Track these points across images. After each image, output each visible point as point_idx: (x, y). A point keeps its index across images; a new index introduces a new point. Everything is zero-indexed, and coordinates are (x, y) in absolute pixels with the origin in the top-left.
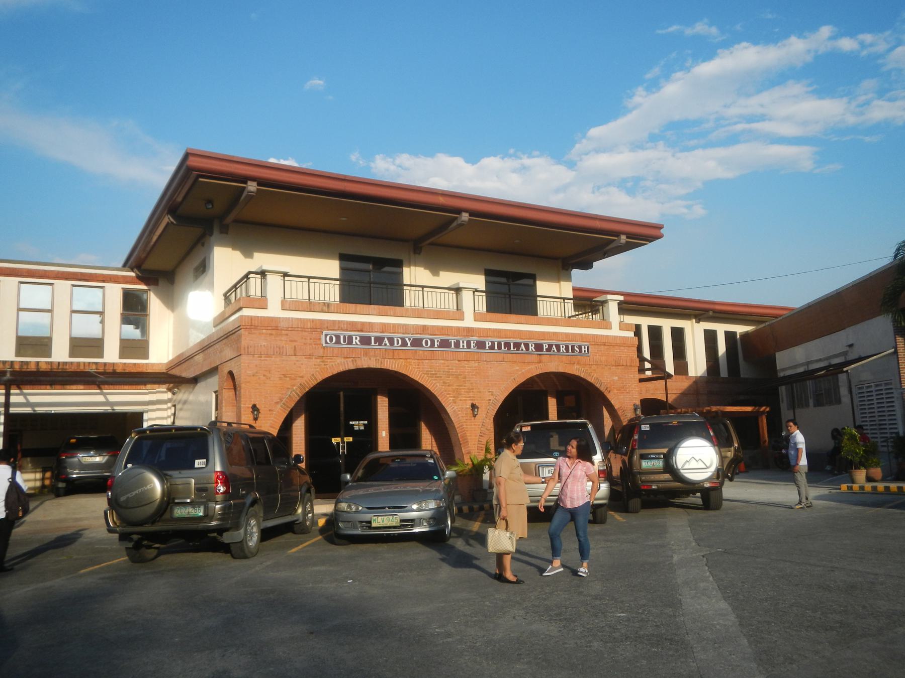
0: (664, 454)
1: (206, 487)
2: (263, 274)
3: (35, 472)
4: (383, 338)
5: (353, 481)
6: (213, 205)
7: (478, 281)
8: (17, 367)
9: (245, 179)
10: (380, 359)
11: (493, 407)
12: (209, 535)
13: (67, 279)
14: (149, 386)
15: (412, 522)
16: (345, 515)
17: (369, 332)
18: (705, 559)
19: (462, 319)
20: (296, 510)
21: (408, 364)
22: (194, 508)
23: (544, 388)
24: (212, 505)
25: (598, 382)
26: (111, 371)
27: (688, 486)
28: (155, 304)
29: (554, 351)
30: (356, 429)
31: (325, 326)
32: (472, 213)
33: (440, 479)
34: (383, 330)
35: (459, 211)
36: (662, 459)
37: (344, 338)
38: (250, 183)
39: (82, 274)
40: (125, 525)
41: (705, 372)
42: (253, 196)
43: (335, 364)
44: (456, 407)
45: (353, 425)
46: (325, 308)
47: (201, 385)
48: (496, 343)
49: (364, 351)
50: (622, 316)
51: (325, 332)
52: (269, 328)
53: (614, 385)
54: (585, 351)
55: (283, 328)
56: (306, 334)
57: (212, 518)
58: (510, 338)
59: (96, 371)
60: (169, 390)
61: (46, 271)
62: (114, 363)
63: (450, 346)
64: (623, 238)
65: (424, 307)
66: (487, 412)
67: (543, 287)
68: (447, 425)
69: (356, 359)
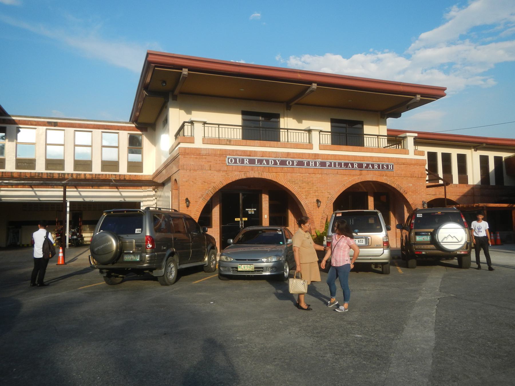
0: (431, 233)
1: (141, 245)
2: (192, 123)
3: (91, 233)
4: (262, 160)
5: (233, 243)
6: (166, 84)
7: (327, 126)
8: (74, 177)
9: (181, 67)
10: (261, 173)
11: (330, 201)
12: (144, 271)
13: (99, 128)
14: (143, 188)
15: (261, 269)
16: (224, 263)
17: (254, 156)
18: (438, 301)
19: (311, 148)
20: (204, 259)
21: (278, 176)
22: (134, 256)
23: (366, 191)
24: (144, 254)
25: (398, 187)
26: (123, 179)
27: (447, 253)
28: (146, 141)
29: (370, 168)
30: (249, 213)
31: (228, 153)
32: (319, 84)
33: (284, 244)
34: (262, 155)
35: (310, 83)
36: (429, 235)
37: (239, 160)
38: (184, 69)
39: (107, 126)
40: (99, 264)
41: (479, 182)
42: (186, 77)
43: (234, 176)
44: (307, 201)
45: (248, 211)
46: (228, 143)
47: (166, 187)
48: (333, 163)
49: (251, 168)
50: (416, 147)
51: (228, 157)
52: (195, 154)
53: (409, 190)
54: (390, 168)
55: (203, 155)
56: (217, 157)
57: (144, 262)
58: (342, 160)
59: (115, 179)
60: (154, 190)
61: (88, 124)
62: (124, 175)
63: (304, 165)
64: (419, 97)
65: (288, 142)
66: (327, 205)
67: (368, 129)
68: (302, 212)
69: (246, 172)
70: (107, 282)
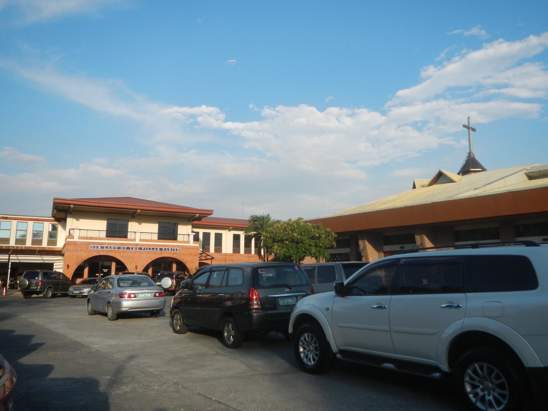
8: (15, 248)
9: (70, 204)
13: (32, 221)
23: (172, 261)
28: (60, 228)
37: (96, 247)
46: (91, 239)
70: (24, 297)
